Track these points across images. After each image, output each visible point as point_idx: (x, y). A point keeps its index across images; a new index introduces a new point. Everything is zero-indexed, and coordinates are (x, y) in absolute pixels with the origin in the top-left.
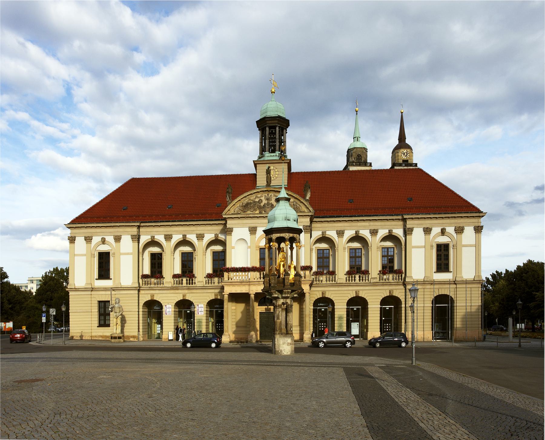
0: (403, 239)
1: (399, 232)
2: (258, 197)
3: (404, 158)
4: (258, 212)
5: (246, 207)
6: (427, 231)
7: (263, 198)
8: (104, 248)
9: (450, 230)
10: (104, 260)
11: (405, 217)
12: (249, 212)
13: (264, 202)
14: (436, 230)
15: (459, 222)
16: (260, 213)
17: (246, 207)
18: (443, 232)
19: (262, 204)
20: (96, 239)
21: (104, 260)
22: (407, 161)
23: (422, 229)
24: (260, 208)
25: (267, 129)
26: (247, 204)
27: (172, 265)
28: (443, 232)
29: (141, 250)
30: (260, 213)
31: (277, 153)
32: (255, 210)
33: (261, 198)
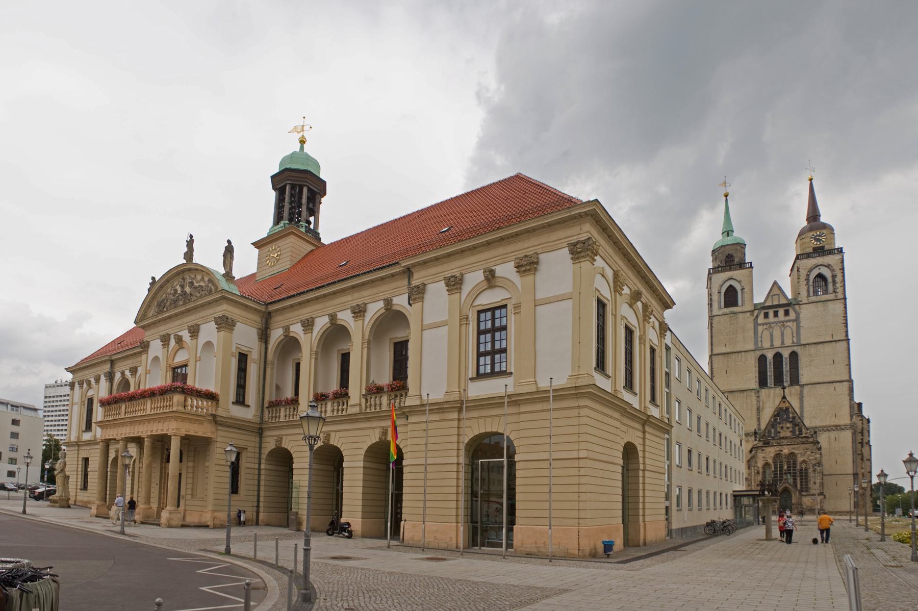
6: (454, 284)
9: (506, 270)
14: (474, 278)
15: (526, 245)
18: (491, 277)
28: (491, 277)
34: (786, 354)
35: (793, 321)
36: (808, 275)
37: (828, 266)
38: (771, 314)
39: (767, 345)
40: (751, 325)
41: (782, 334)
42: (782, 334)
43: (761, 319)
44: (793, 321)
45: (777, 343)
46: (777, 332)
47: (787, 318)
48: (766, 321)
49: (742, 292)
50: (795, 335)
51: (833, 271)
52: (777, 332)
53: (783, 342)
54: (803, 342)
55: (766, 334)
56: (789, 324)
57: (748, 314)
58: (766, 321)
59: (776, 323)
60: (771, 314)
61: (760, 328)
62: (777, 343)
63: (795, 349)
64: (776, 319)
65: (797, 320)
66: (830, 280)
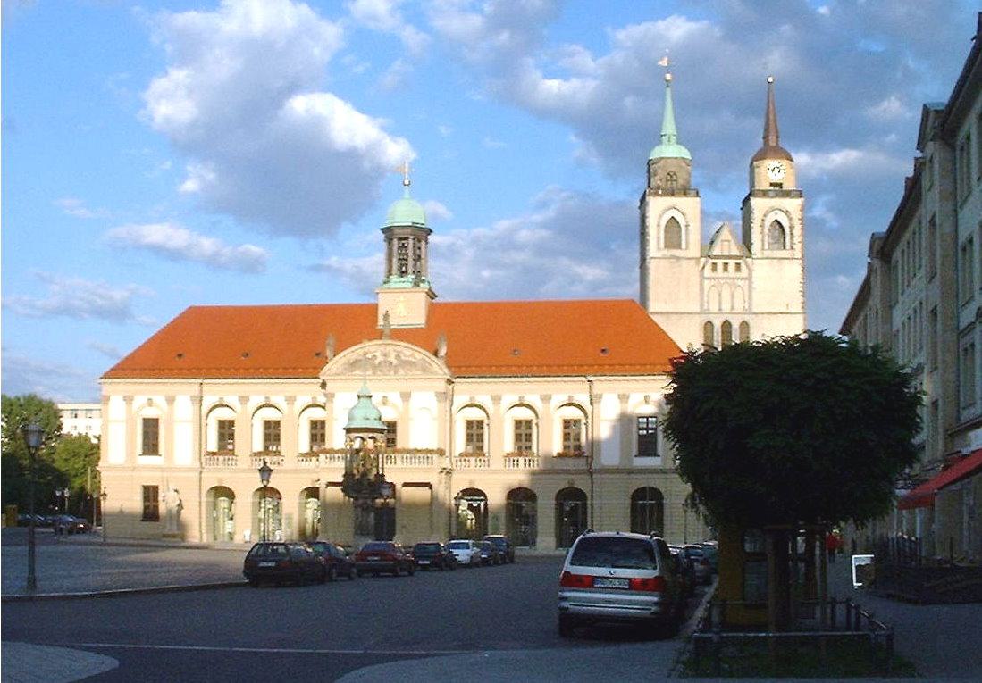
0: (588, 408)
1: (583, 399)
2: (371, 353)
3: (776, 180)
4: (370, 372)
5: (354, 365)
7: (378, 354)
8: (150, 413)
10: (151, 431)
11: (590, 379)
12: (357, 372)
13: (380, 358)
16: (374, 373)
17: (354, 365)
19: (377, 362)
20: (140, 400)
21: (151, 431)
22: (780, 185)
23: (616, 396)
24: (375, 367)
25: (395, 242)
26: (355, 362)
27: (251, 438)
29: (204, 418)
30: (374, 373)
31: (411, 277)
32: (367, 370)
33: (375, 354)
34: (736, 325)
35: (746, 279)
36: (763, 220)
37: (786, 212)
38: (720, 267)
39: (714, 308)
40: (696, 279)
41: (732, 296)
42: (732, 296)
43: (708, 272)
44: (746, 279)
45: (726, 307)
46: (726, 294)
47: (738, 275)
48: (714, 275)
49: (687, 230)
50: (747, 299)
51: (790, 219)
52: (726, 294)
53: (732, 308)
54: (755, 310)
55: (714, 294)
56: (739, 282)
57: (694, 261)
58: (714, 275)
59: (727, 278)
60: (720, 267)
61: (707, 283)
62: (726, 307)
63: (746, 318)
64: (726, 274)
65: (749, 278)
66: (787, 230)
